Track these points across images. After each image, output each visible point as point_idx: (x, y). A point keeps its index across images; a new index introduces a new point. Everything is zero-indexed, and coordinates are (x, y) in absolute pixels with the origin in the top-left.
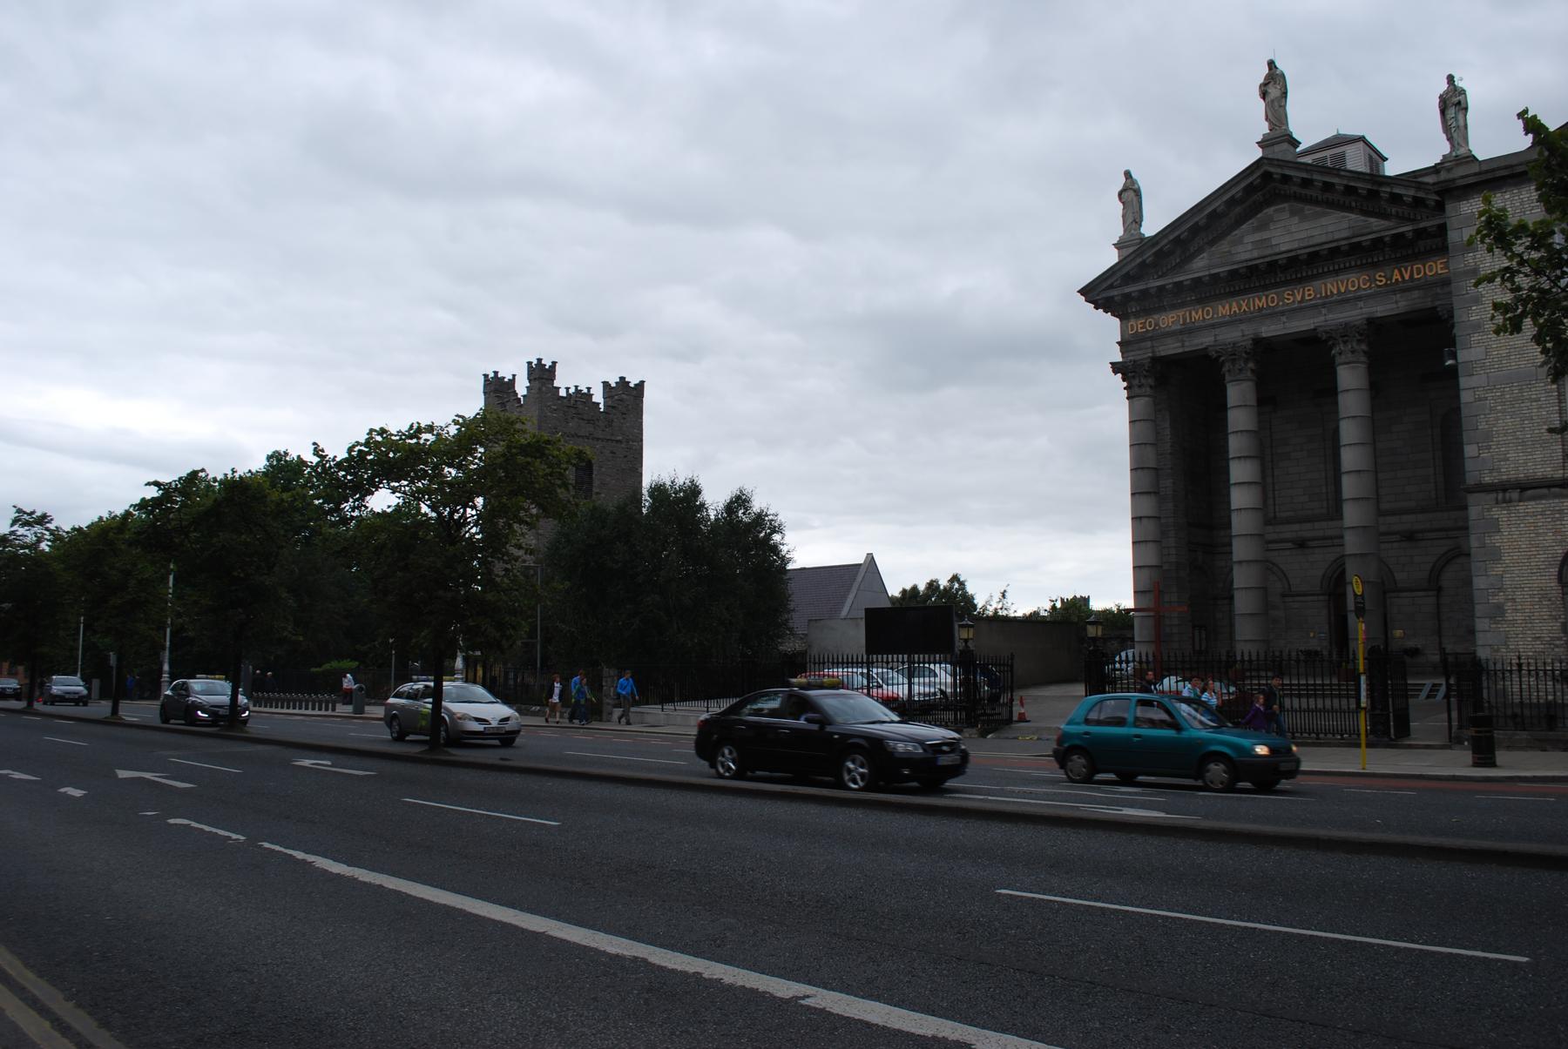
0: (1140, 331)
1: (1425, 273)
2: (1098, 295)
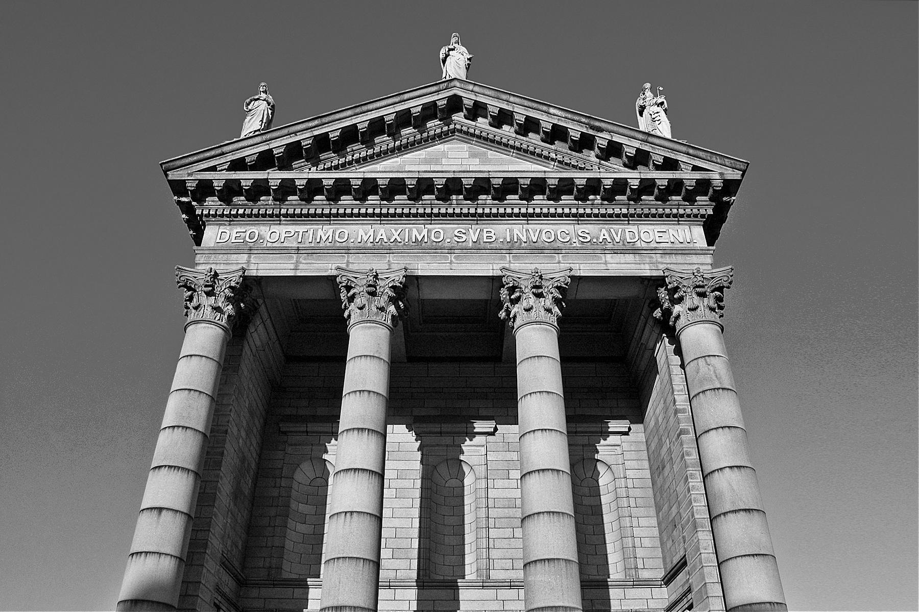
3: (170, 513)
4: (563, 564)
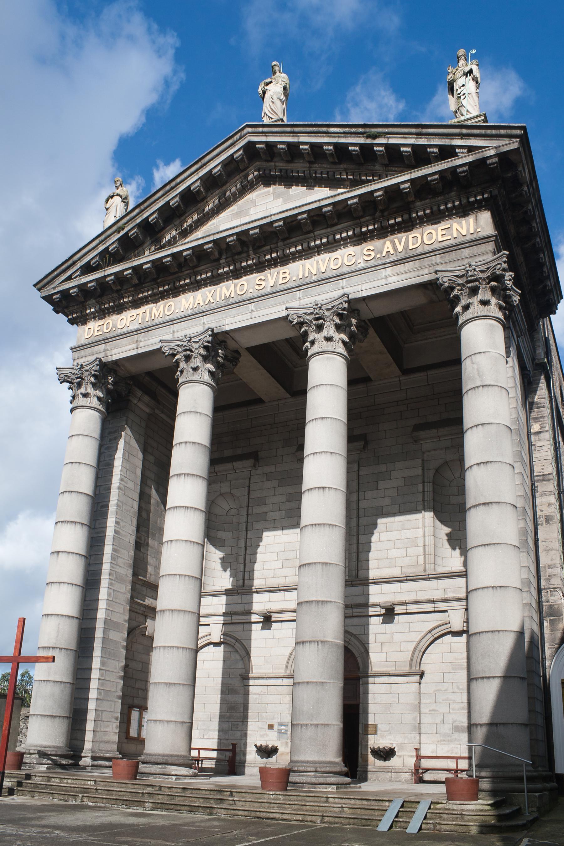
1: (423, 242)
2: (54, 288)
3: (64, 554)
4: (319, 567)
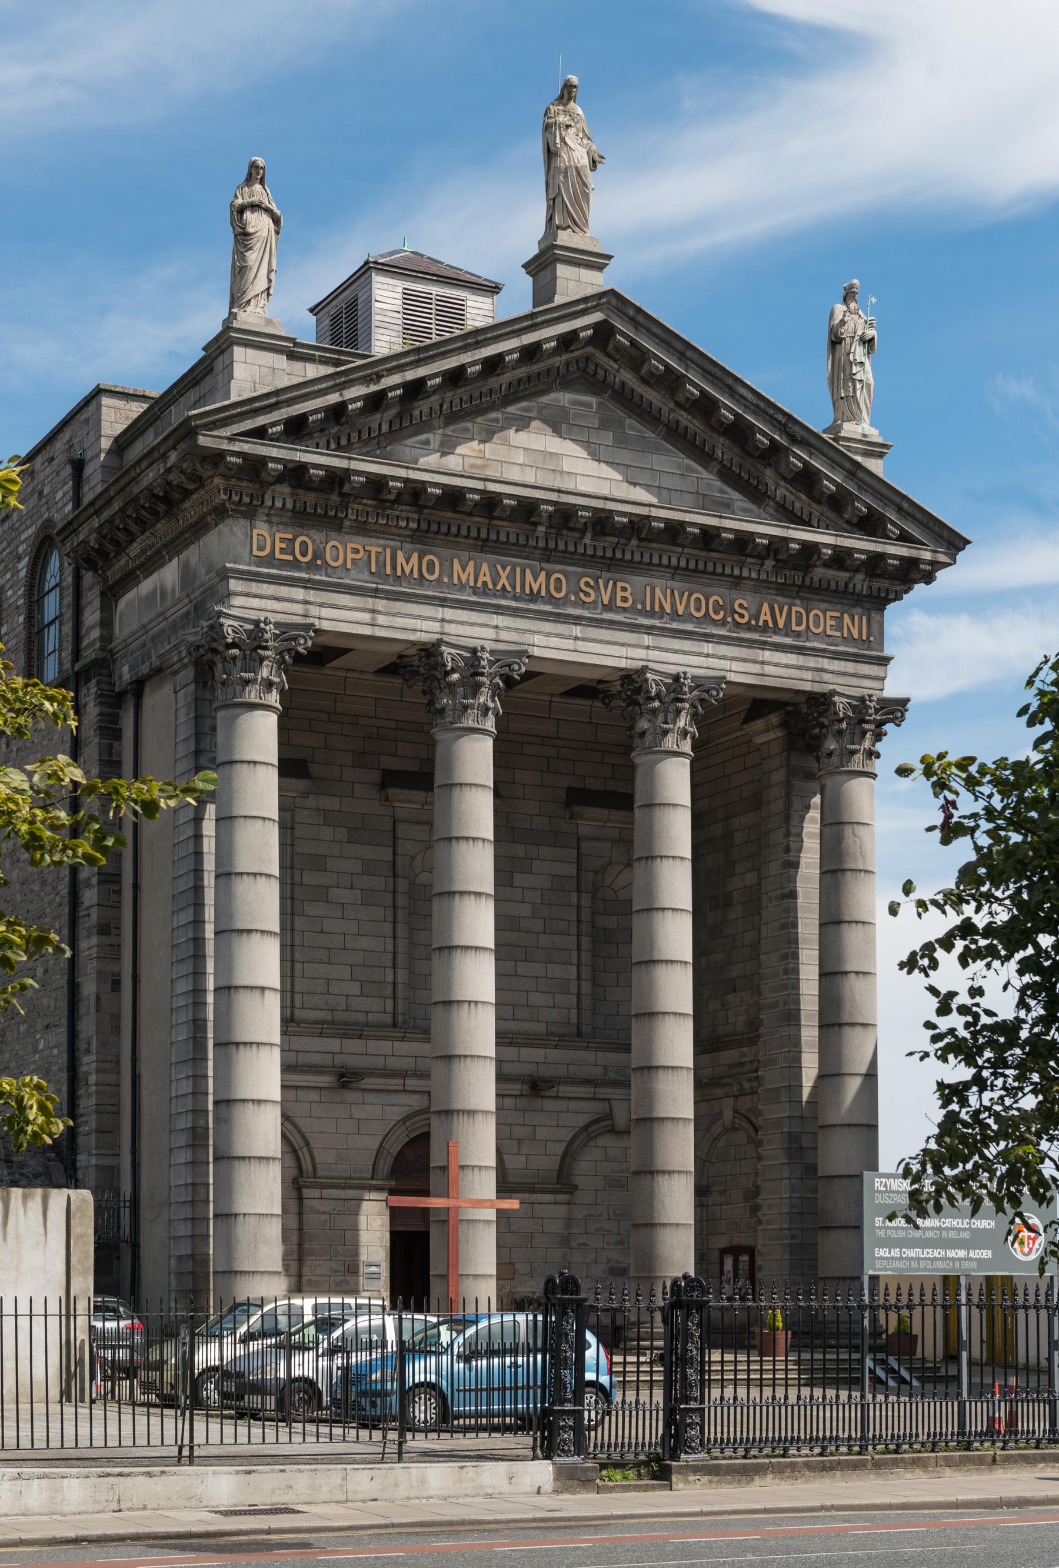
0: (278, 555)
2: (231, 439)
